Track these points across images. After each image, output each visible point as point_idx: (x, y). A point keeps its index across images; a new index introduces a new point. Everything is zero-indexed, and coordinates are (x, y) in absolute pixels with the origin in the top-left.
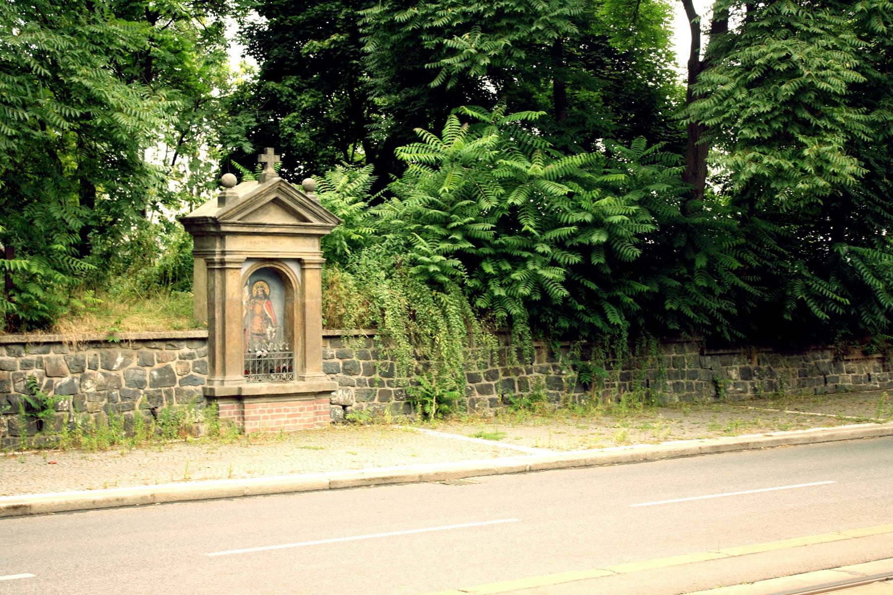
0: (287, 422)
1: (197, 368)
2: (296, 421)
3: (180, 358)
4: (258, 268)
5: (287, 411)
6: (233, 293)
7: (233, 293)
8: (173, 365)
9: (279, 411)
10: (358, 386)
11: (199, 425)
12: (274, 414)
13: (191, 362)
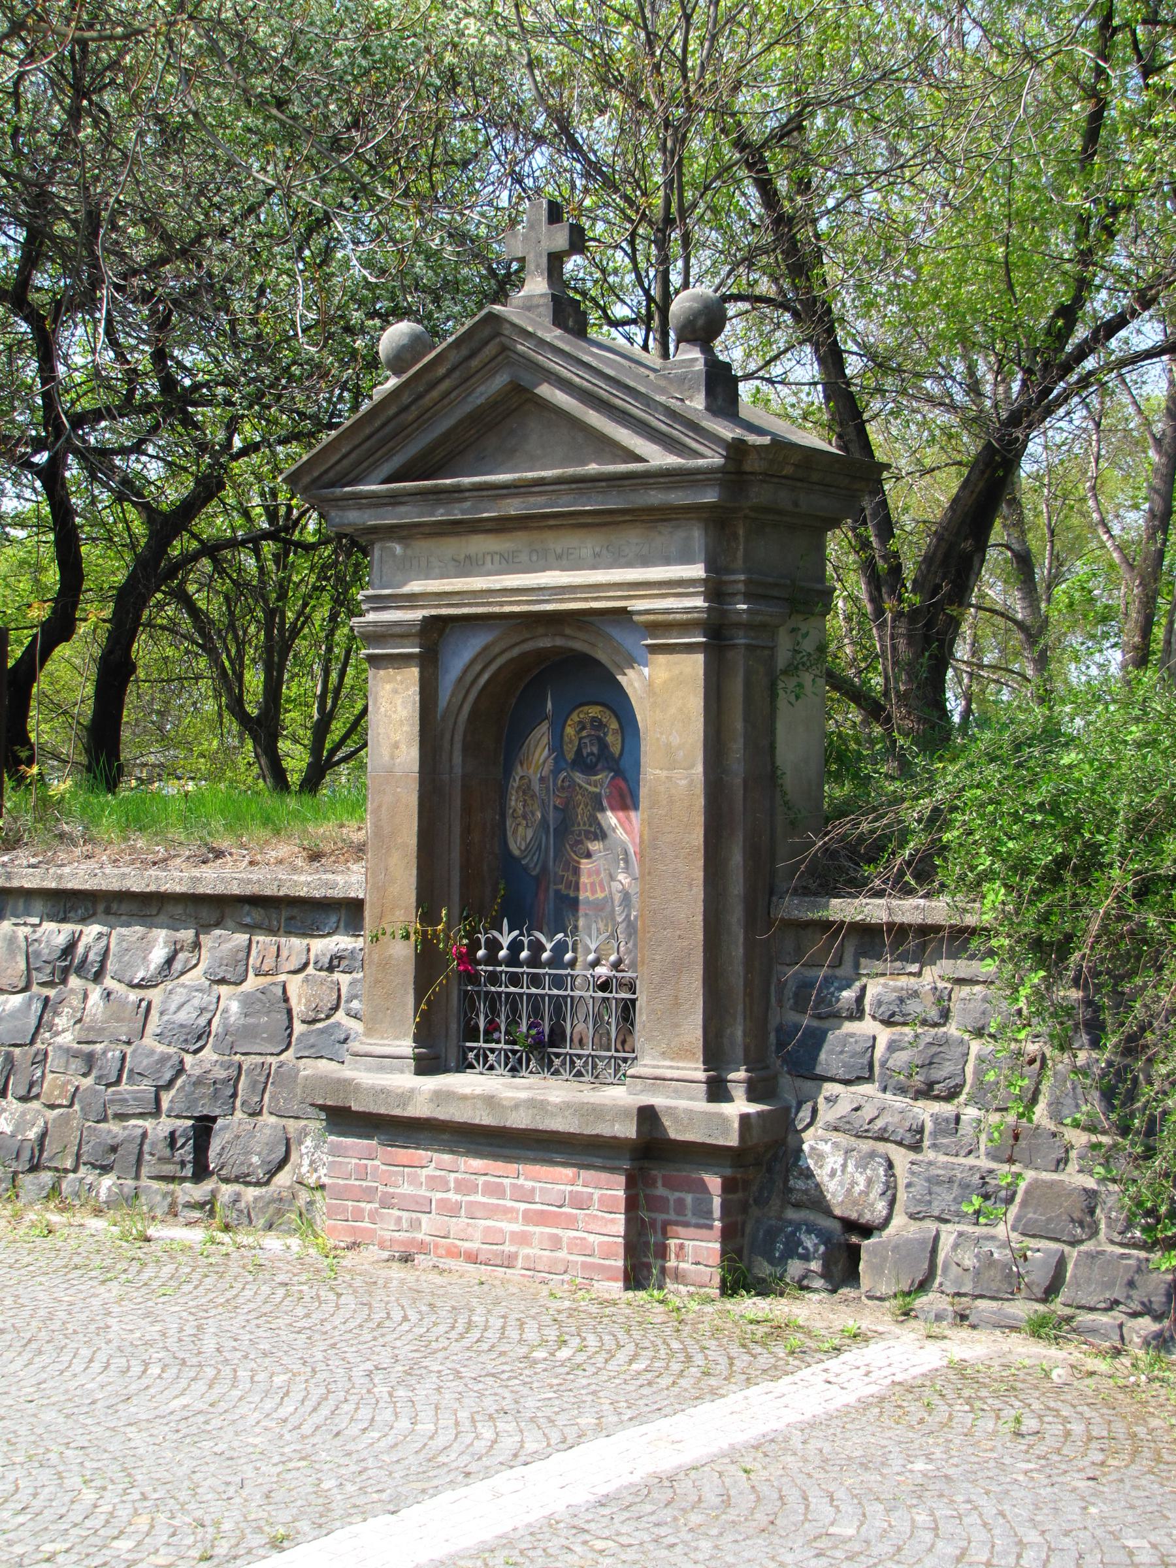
0: (523, 1239)
2: (556, 1243)
4: (515, 652)
5: (526, 1196)
6: (396, 746)
7: (396, 746)
12: (479, 1198)
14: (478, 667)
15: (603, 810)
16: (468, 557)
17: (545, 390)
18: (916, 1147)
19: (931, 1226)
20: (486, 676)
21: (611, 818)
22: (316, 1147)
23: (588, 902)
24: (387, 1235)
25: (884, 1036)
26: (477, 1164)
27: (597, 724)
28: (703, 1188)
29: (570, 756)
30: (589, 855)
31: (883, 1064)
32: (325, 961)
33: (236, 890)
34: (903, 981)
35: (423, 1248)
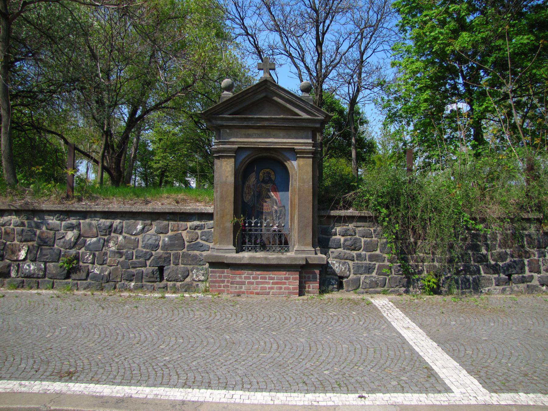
0: (272, 288)
1: (204, 237)
2: (281, 288)
3: (190, 228)
4: (256, 156)
5: (273, 279)
6: (227, 177)
7: (227, 177)
8: (184, 234)
9: (265, 278)
10: (357, 260)
11: (198, 283)
12: (259, 280)
13: (199, 232)
14: (246, 159)
15: (270, 192)
16: (248, 134)
17: (275, 98)
18: (353, 260)
19: (359, 275)
20: (248, 162)
21: (272, 194)
22: (197, 272)
23: (266, 212)
24: (233, 291)
25: (342, 239)
26: (258, 272)
27: (269, 173)
28: (315, 273)
29: (261, 180)
30: (266, 202)
31: (344, 244)
32: (194, 227)
33: (167, 211)
34: (345, 227)
35: (243, 293)
